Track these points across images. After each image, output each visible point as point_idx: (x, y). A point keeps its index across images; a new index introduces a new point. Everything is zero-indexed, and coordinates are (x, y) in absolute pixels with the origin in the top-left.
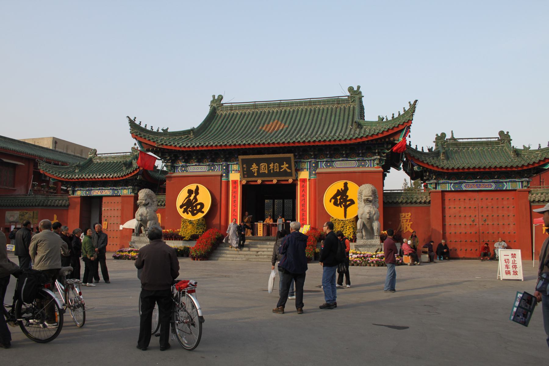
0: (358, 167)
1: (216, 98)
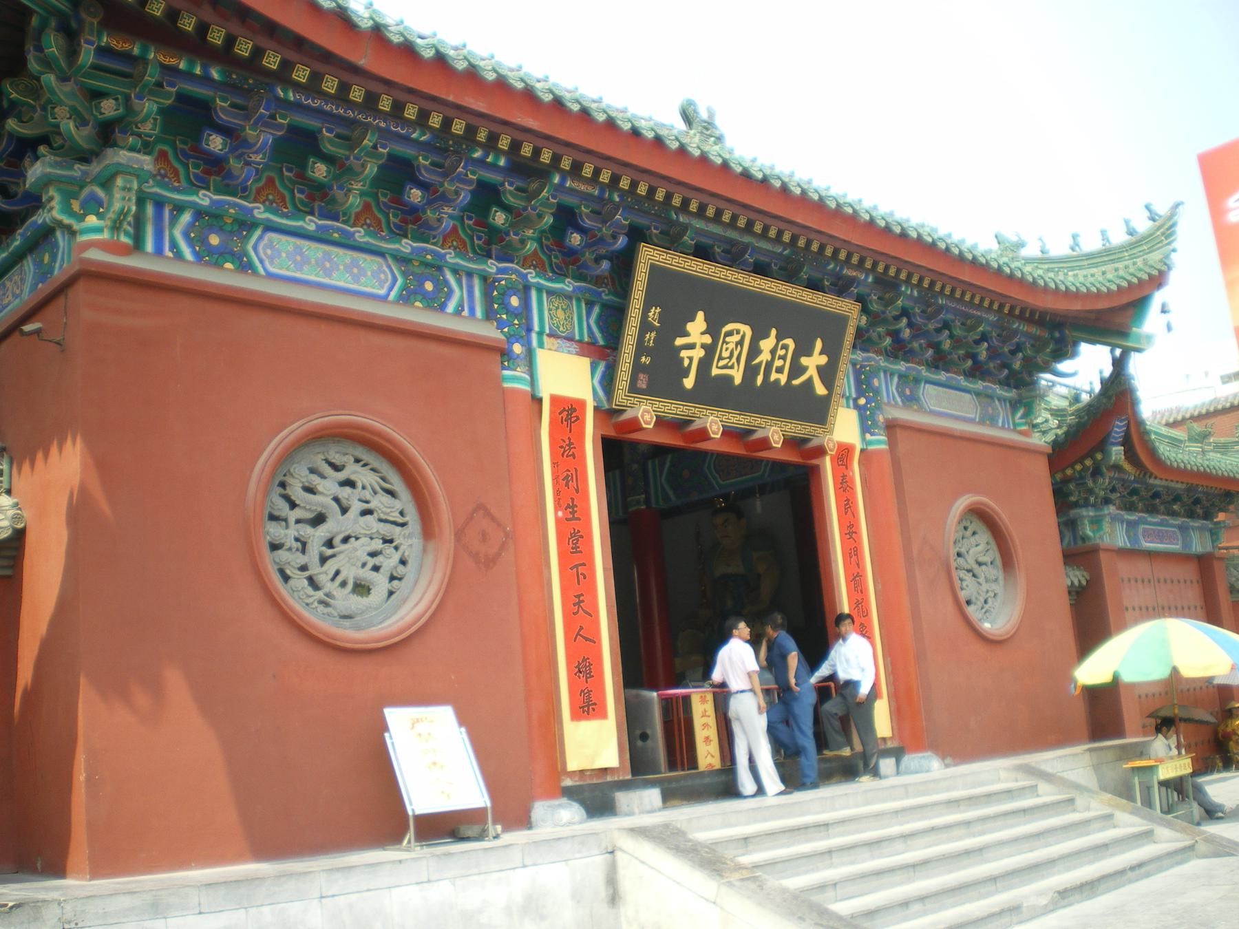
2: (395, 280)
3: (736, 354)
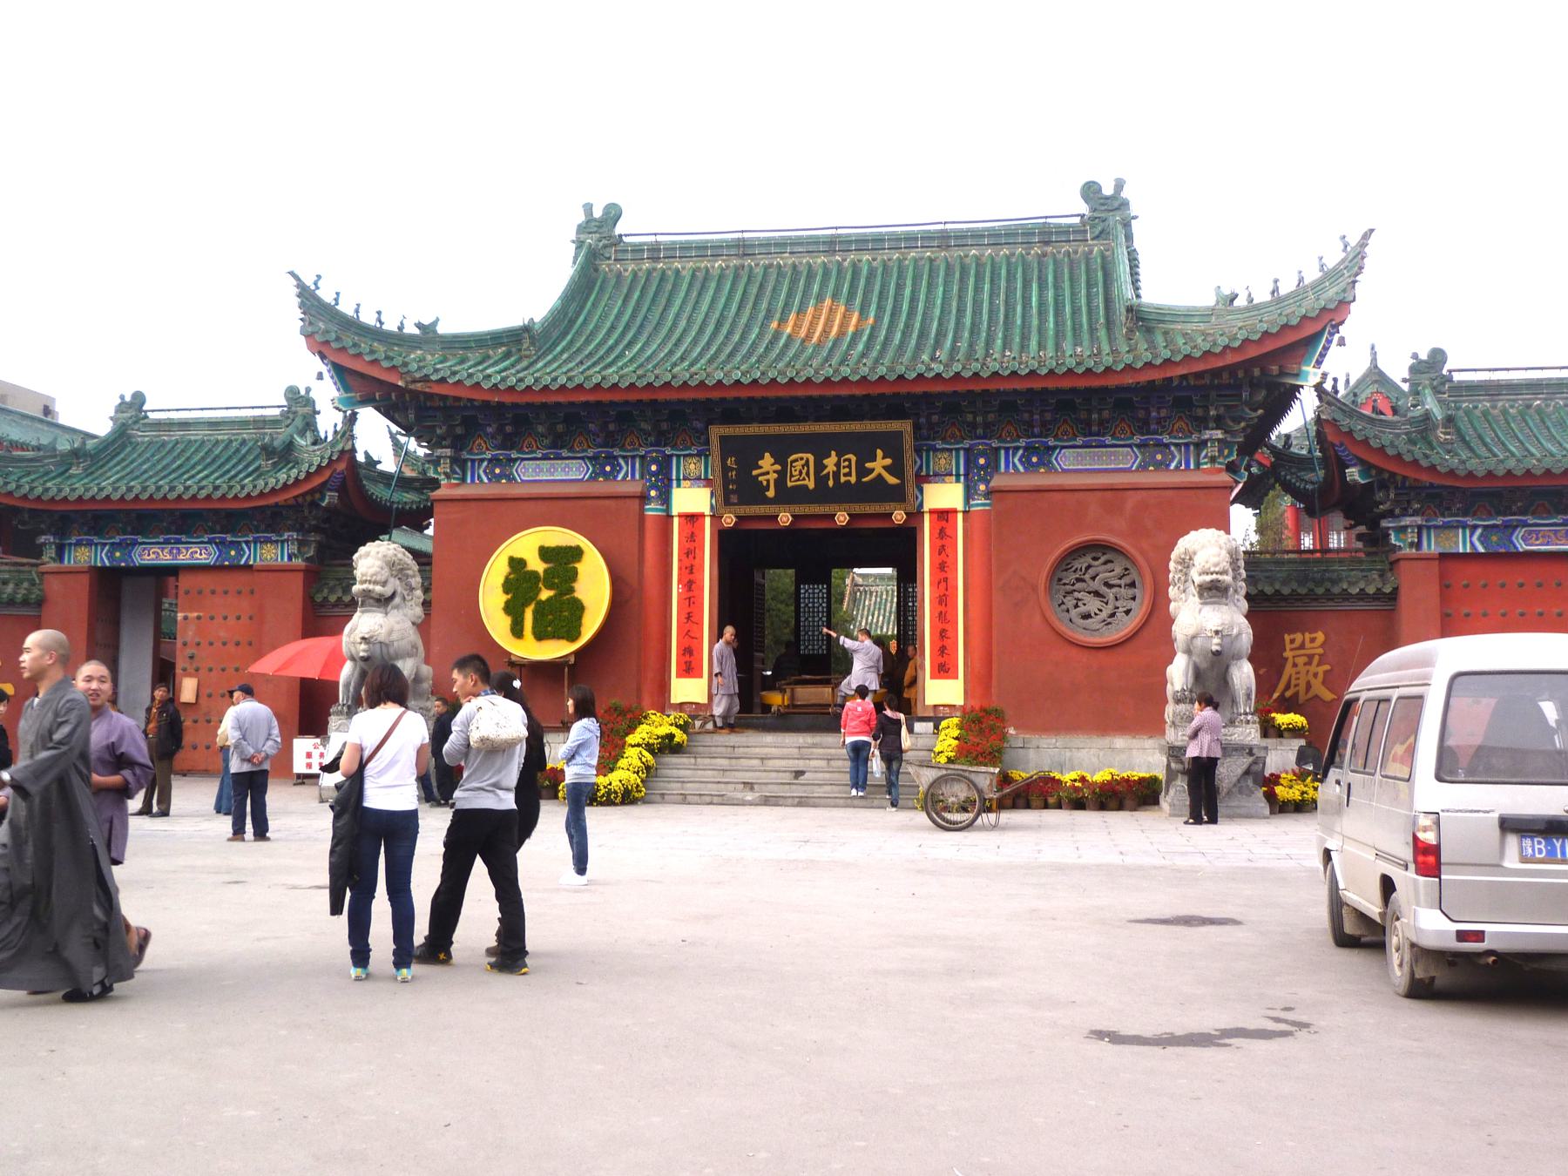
0: (1143, 468)
1: (597, 213)
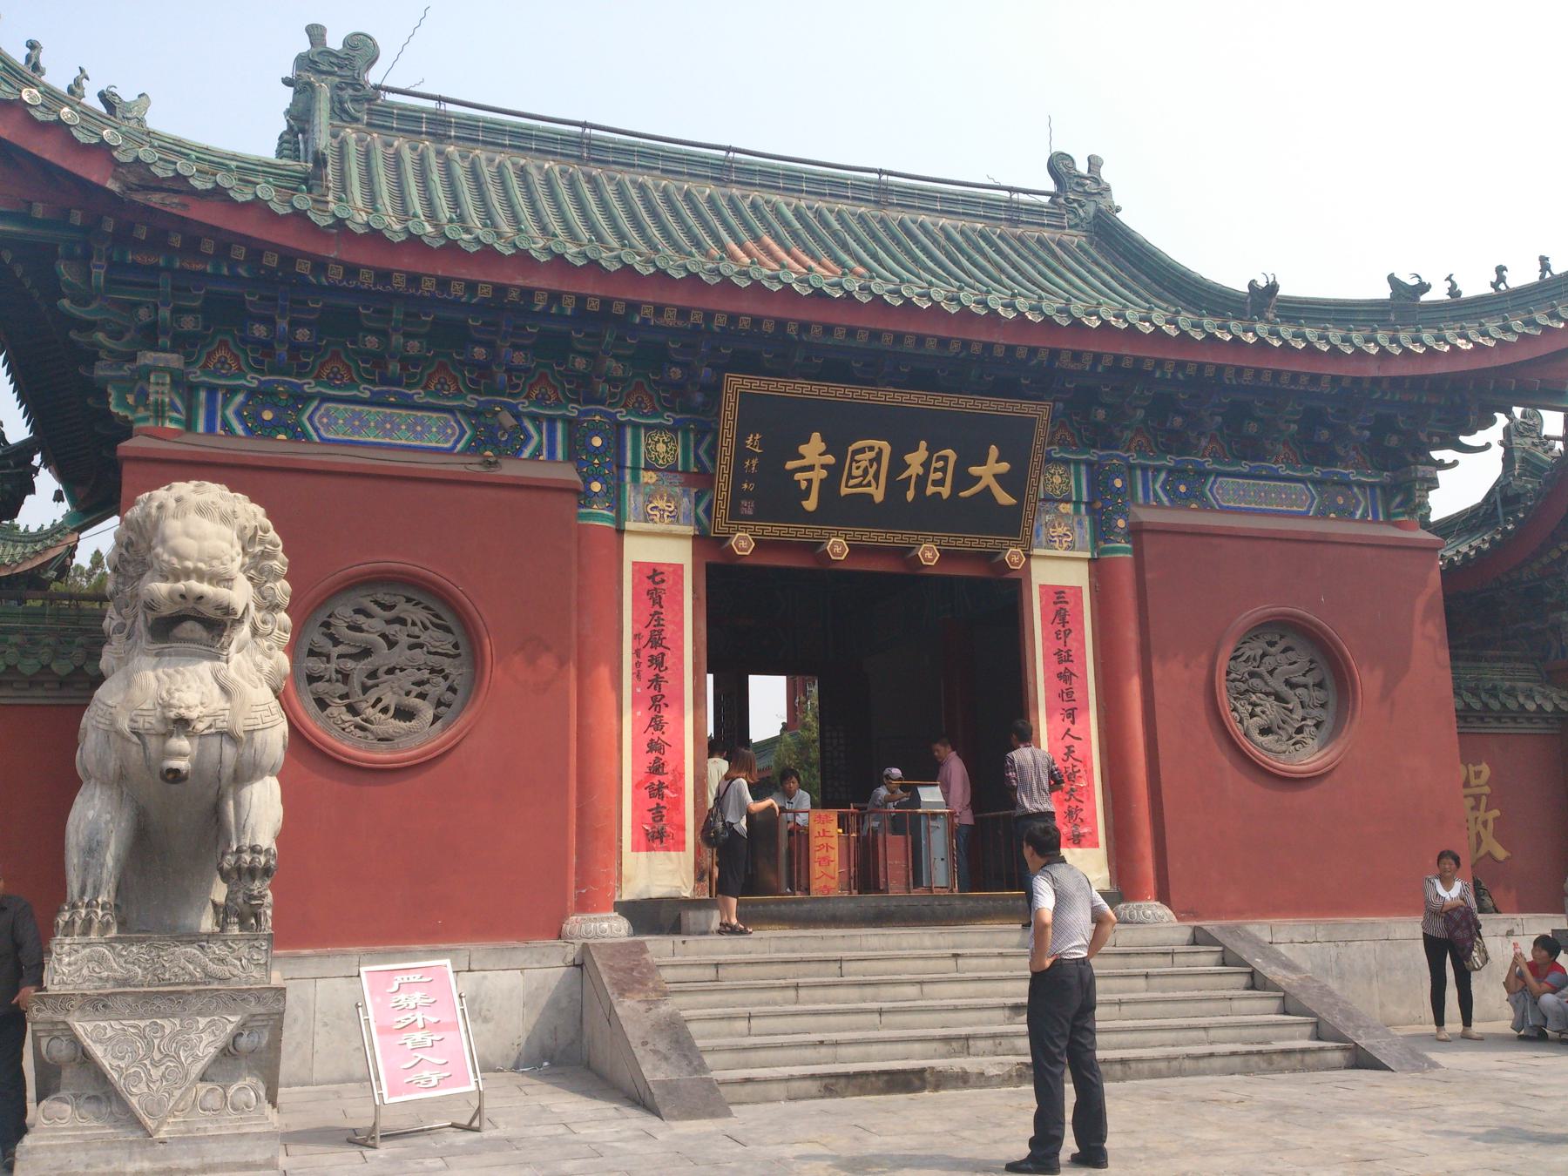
0: (1322, 514)
1: (335, 42)
2: (463, 432)
3: (872, 471)
